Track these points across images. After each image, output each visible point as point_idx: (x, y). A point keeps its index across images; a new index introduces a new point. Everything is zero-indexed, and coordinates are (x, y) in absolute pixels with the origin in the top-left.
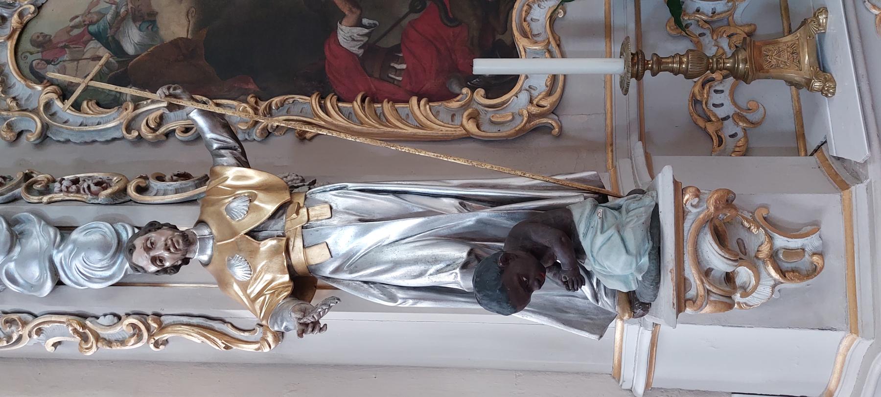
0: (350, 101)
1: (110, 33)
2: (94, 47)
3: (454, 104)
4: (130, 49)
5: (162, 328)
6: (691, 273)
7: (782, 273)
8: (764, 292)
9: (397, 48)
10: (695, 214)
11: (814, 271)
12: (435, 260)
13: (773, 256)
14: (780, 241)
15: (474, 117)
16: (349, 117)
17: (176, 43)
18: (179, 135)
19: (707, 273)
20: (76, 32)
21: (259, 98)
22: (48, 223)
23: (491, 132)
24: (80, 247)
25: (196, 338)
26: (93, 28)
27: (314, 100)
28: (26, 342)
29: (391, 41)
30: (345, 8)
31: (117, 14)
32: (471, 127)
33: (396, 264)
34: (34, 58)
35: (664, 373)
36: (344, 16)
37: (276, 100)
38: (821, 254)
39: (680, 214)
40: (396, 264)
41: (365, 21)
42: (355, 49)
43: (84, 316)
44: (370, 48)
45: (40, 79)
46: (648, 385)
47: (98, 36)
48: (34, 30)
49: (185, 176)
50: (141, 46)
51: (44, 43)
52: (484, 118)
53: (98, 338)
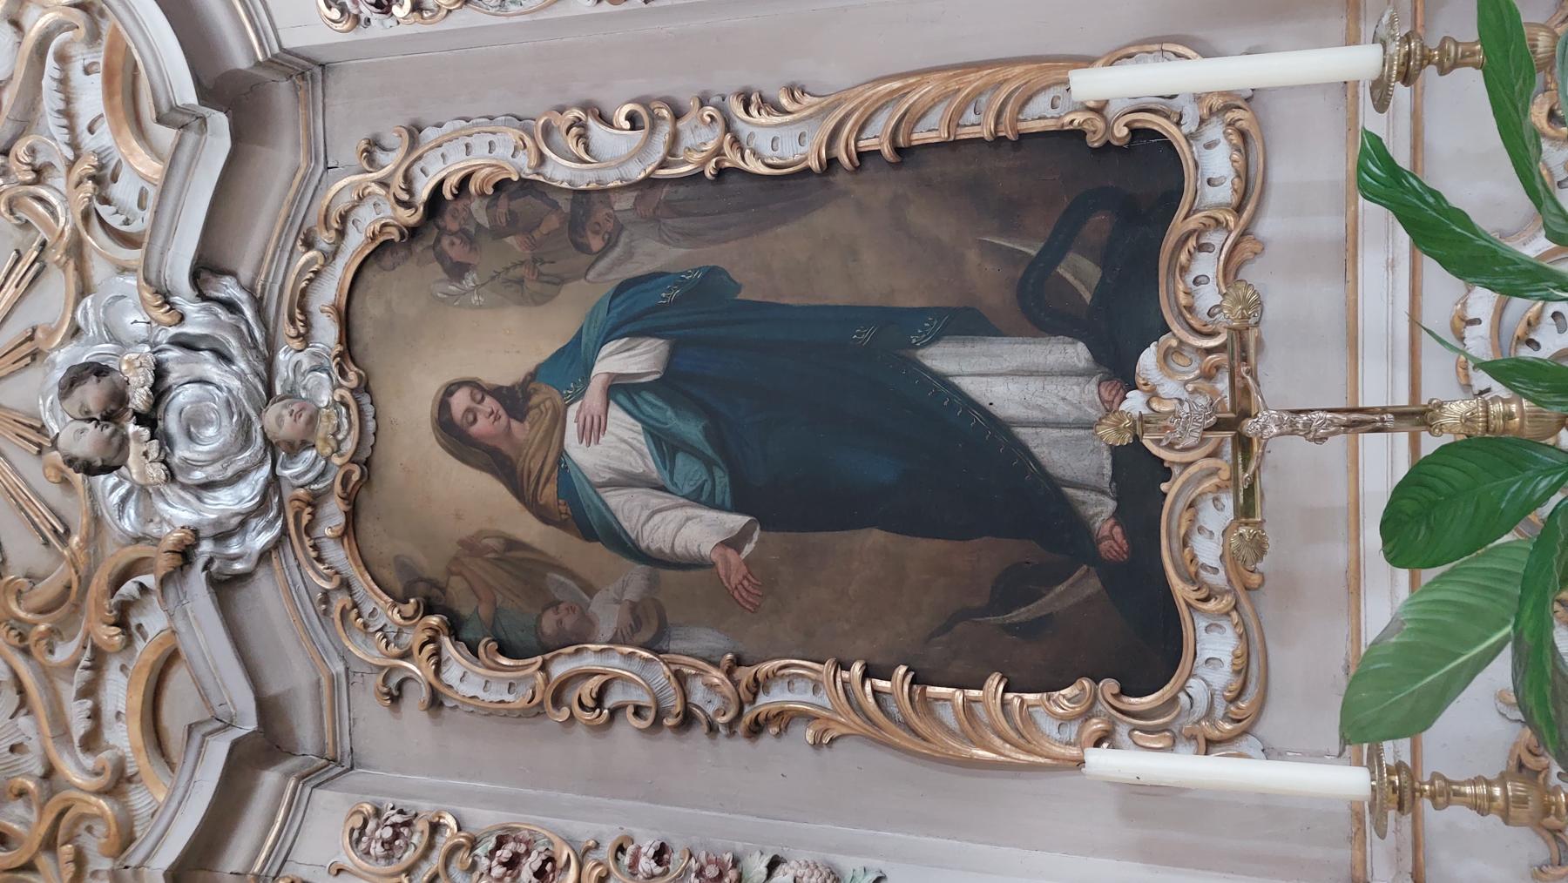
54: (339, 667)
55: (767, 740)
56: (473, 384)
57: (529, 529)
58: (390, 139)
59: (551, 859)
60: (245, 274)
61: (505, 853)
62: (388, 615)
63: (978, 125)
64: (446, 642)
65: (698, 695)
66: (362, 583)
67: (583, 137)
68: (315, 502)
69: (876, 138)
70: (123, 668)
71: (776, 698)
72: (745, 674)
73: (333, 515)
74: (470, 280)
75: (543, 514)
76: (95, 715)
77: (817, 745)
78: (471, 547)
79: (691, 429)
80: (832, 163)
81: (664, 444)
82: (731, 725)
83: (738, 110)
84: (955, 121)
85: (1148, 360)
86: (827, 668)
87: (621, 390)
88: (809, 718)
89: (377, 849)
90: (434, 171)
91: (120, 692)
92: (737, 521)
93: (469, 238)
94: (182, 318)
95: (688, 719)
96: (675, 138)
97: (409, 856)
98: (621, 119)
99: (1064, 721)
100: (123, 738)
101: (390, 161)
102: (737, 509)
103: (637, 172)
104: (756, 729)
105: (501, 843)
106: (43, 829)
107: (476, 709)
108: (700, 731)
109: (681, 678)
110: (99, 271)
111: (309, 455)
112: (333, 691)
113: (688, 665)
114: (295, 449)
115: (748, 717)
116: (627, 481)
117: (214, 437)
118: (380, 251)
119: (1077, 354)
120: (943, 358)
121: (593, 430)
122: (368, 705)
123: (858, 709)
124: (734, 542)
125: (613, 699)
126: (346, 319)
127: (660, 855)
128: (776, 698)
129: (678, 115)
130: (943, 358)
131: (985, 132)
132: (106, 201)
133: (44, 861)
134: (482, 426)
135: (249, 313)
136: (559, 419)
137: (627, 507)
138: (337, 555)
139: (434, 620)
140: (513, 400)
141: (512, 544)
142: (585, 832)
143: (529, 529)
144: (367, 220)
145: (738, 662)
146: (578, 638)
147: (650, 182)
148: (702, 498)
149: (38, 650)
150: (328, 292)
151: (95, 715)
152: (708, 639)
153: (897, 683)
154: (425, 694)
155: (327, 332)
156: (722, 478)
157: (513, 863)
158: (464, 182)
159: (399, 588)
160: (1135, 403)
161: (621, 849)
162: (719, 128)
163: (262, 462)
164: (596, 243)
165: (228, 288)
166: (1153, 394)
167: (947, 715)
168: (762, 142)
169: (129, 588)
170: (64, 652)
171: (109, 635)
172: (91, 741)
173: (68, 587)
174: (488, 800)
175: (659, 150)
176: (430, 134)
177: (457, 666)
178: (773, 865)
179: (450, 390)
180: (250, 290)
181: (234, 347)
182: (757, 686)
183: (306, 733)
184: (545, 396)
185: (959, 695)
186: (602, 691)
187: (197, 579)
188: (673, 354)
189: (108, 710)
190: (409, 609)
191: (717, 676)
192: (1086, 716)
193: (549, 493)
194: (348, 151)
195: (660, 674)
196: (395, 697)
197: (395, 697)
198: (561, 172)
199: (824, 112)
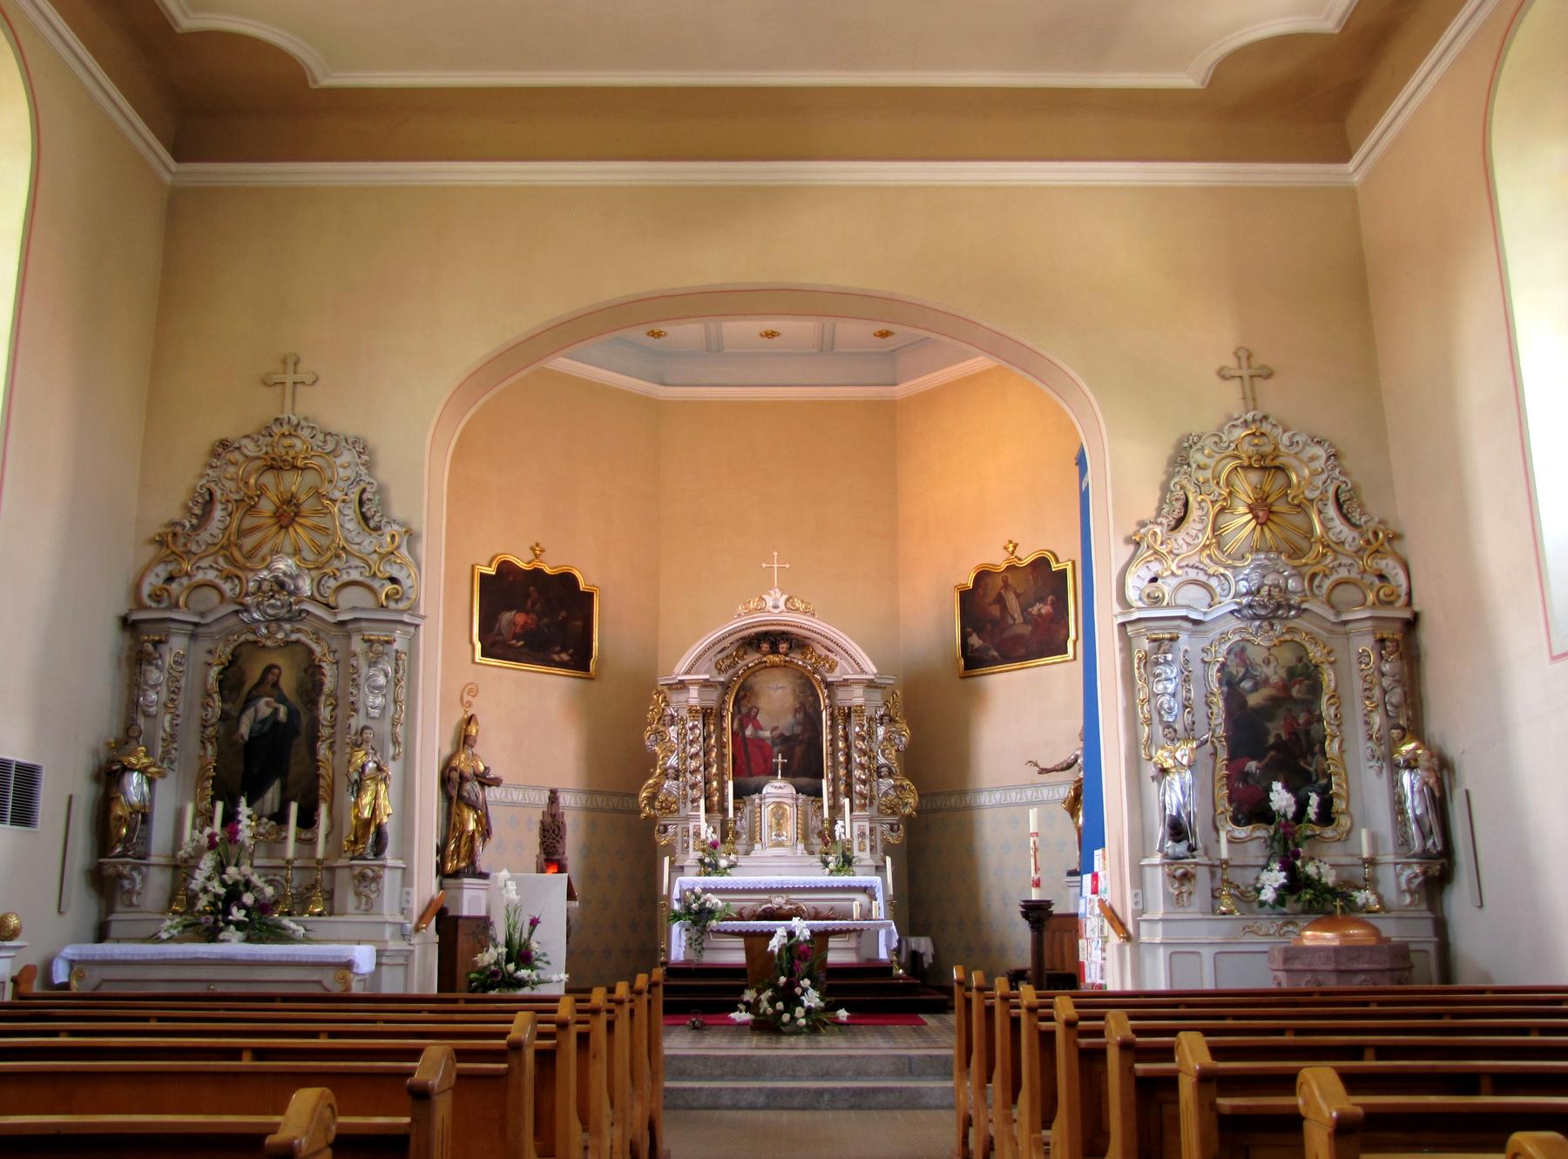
0: (1227, 770)
1: (1248, 675)
2: (1242, 671)
3: (1227, 806)
4: (1242, 685)
5: (1147, 725)
6: (1175, 866)
7: (1177, 895)
8: (1172, 891)
9: (1248, 784)
10: (1188, 868)
11: (1178, 903)
12: (1172, 807)
13: (1181, 893)
14: (1185, 895)
15: (1223, 813)
16: (1221, 769)
17: (1245, 702)
18: (1210, 711)
19: (1175, 870)
20: (1248, 662)
21: (1225, 737)
22: (1175, 689)
23: (1218, 818)
24: (1169, 701)
25: (1145, 736)
26: (1250, 668)
27: (1226, 757)
28: (1140, 683)
29: (1251, 781)
30: (1265, 761)
31: (1256, 676)
32: (1219, 811)
33: (1171, 797)
34: (1237, 649)
35: (1147, 870)
36: (1260, 762)
37: (1224, 743)
38: (1183, 906)
39: (1189, 864)
40: (1171, 797)
41: (1258, 771)
42: (1247, 769)
43: (1149, 701)
44: (1248, 774)
45: (1228, 653)
46: (1142, 865)
47: (1247, 671)
48: (1249, 646)
49: (1194, 723)
50: (1244, 689)
51: (1243, 650)
52: (1222, 816)
53: (1143, 705)
54: (217, 637)
55: (200, 744)
56: (280, 674)
57: (247, 687)
58: (337, 655)
59: (175, 700)
60: (308, 617)
61: (176, 690)
62: (228, 650)
63: (321, 792)
64: (221, 667)
65: (211, 729)
66: (236, 644)
67: (329, 705)
68: (255, 633)
69: (322, 771)
70: (217, 576)
71: (209, 747)
72: (214, 740)
73: (251, 637)
74: (303, 674)
75: (250, 692)
76: (206, 568)
77: (201, 756)
78: (243, 673)
79: (266, 728)
80: (318, 761)
81: (263, 721)
82: (203, 737)
83: (331, 740)
84: (323, 787)
85: (273, 823)
86: (215, 758)
87: (276, 711)
88: (205, 753)
89: (176, 659)
90: (328, 669)
91: (211, 575)
92: (246, 738)
93: (313, 674)
94: (296, 605)
95: (205, 727)
96: (328, 727)
97: (174, 666)
98: (333, 713)
99: (205, 806)
100: (200, 577)
101: (330, 658)
102: (249, 738)
103: (321, 718)
104: (202, 742)
105: (178, 688)
106: (177, 552)
107: (206, 676)
108: (202, 729)
109: (213, 725)
110: (314, 573)
111: (266, 631)
112: (210, 636)
113: (217, 727)
114: (267, 628)
115: (206, 741)
116: (256, 712)
117: (270, 611)
118: (311, 652)
119: (276, 810)
120: (277, 784)
121: (268, 704)
122: (209, 645)
123: (207, 764)
124: (242, 737)
125: (210, 709)
126: (298, 642)
127: (177, 725)
128: (209, 747)
129: (332, 727)
130: (277, 784)
131: (321, 793)
132: (329, 577)
133: (169, 551)
134: (270, 677)
135: (299, 618)
136: (270, 696)
137: (250, 712)
138: (243, 638)
139: (227, 664)
140: (276, 685)
141: (244, 684)
142: (181, 706)
143: (247, 687)
144: (318, 650)
145: (217, 738)
146: (223, 701)
147: (319, 721)
148: (251, 731)
149: (221, 552)
150: (303, 638)
151: (206, 568)
152: (221, 732)
153: (212, 773)
154: (211, 661)
155: (294, 637)
156: (255, 735)
157: (174, 692)
158: (323, 674)
159: (236, 653)
160: (265, 820)
161: (178, 716)
162: (327, 736)
163: (264, 618)
164: (309, 706)
165: (304, 615)
166: (266, 824)
167: (205, 783)
168: (324, 746)
169: (236, 581)
170: (221, 561)
171: (225, 573)
172: (199, 568)
173: (238, 563)
174: (187, 681)
175: (325, 723)
176: (335, 667)
177: (216, 669)
178: (175, 749)
179: (279, 668)
180: (305, 618)
181: (291, 615)
182: (212, 743)
183: (201, 630)
184: (276, 692)
185: (209, 785)
186: (211, 707)
187: (237, 607)
188: (282, 724)
189: (206, 571)
190: (230, 657)
191: (214, 733)
192: (206, 810)
193: (255, 693)
194: (334, 646)
195: (214, 720)
196: (210, 652)
197: (210, 652)
198: (323, 698)
199: (328, 760)
